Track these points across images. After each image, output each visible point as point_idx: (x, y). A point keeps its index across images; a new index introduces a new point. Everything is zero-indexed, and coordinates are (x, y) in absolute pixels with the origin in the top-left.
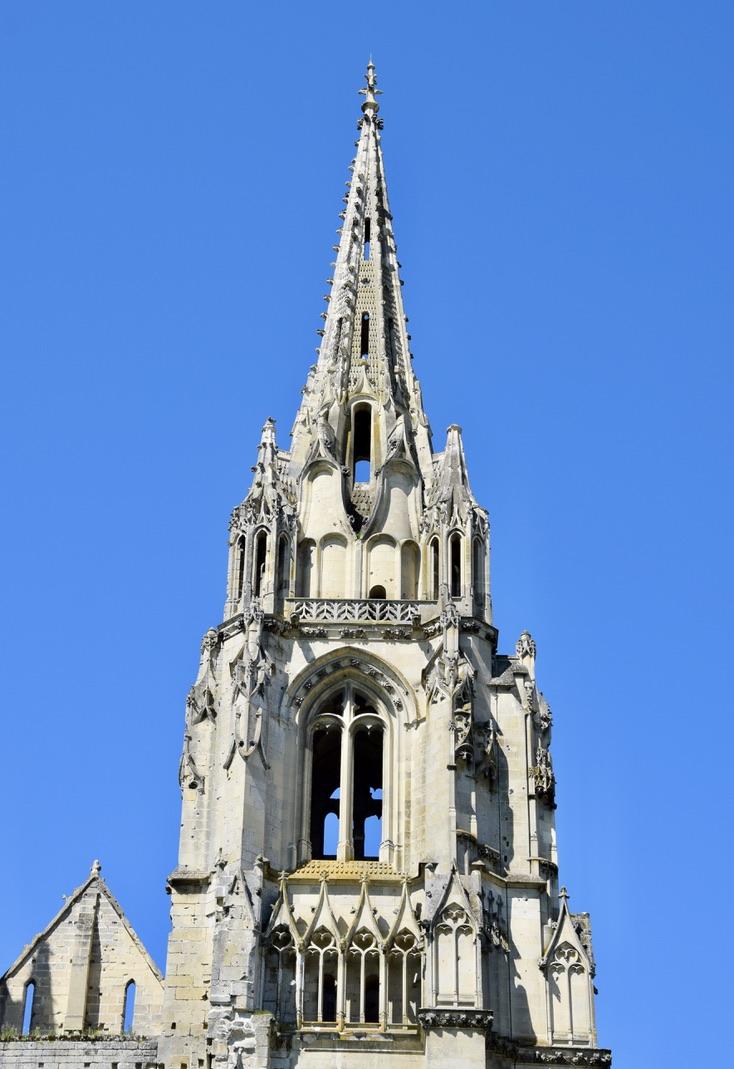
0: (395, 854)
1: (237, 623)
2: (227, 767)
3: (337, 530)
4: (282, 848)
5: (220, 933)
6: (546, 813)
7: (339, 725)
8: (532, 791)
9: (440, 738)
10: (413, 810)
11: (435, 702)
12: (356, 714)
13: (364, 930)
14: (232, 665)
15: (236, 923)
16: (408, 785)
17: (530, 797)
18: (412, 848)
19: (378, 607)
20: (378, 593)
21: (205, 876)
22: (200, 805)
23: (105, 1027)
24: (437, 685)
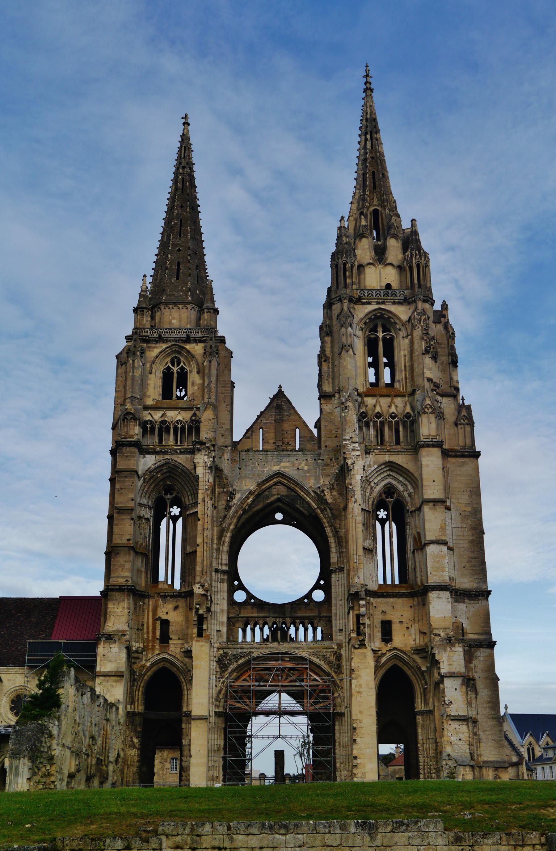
2: (340, 354)
3: (371, 261)
6: (455, 369)
8: (450, 361)
13: (393, 413)
14: (338, 316)
15: (350, 412)
16: (405, 360)
17: (449, 364)
18: (408, 383)
19: (390, 292)
20: (388, 286)
22: (329, 368)
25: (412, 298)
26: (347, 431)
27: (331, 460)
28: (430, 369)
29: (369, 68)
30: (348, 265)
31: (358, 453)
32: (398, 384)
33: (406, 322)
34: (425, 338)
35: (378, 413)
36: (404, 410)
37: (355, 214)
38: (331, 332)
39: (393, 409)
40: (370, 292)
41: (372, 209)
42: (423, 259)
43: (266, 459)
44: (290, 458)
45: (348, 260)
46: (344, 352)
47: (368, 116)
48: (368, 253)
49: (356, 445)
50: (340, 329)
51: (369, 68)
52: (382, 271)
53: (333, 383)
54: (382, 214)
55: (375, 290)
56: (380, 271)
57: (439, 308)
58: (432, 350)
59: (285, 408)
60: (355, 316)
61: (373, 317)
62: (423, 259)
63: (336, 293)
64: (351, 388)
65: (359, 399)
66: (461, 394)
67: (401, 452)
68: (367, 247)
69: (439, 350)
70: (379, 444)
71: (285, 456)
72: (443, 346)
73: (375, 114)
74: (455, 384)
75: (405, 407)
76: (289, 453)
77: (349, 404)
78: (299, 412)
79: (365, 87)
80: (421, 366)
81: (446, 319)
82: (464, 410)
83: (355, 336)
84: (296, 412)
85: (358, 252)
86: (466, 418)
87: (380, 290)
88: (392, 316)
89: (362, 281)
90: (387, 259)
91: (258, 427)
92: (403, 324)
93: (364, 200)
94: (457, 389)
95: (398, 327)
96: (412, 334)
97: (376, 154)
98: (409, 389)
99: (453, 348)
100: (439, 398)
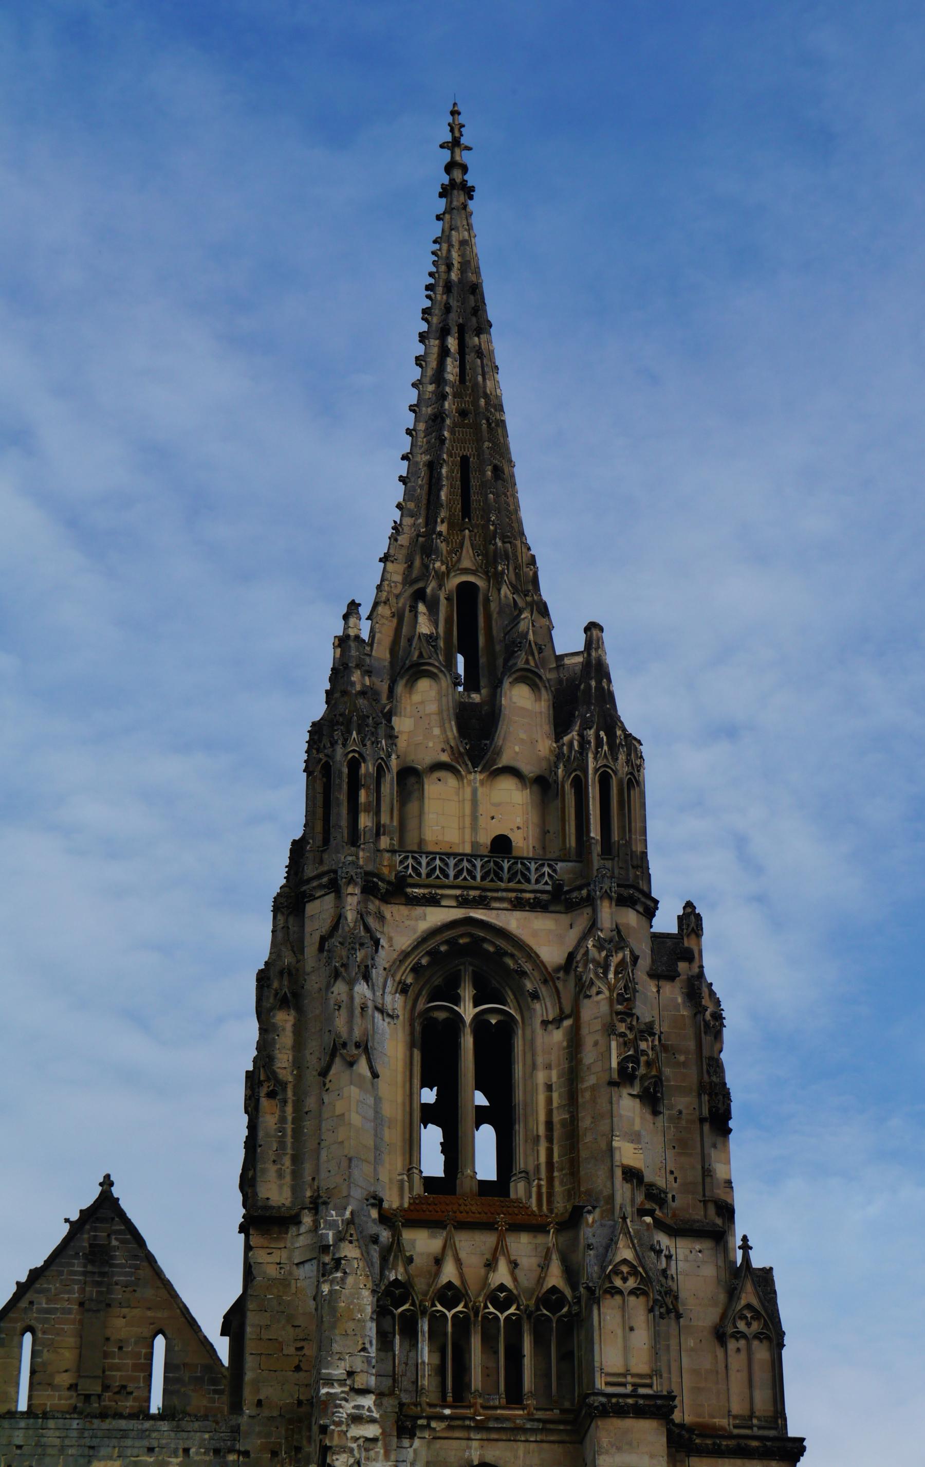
0: (534, 1190)
1: (325, 880)
2: (324, 1073)
3: (445, 758)
4: (390, 1180)
5: (330, 1292)
6: (719, 1140)
7: (459, 1018)
8: (705, 1112)
9: (596, 1044)
10: (556, 1134)
11: (589, 997)
12: (475, 1006)
13: (502, 1287)
14: (323, 940)
15: (350, 1280)
16: (549, 1101)
17: (702, 1120)
18: (557, 1183)
19: (506, 865)
20: (501, 844)
21: (293, 1212)
22: (282, 1120)
23: (129, 1389)
24: (592, 976)
25: (580, 888)
26: (336, 1347)
27: (274, 1454)
28: (635, 1138)
29: (461, 119)
30: (367, 768)
31: (372, 1431)
32: (521, 1186)
33: (558, 969)
34: (622, 1028)
35: (450, 1285)
36: (541, 1280)
37: (398, 597)
38: (296, 995)
39: (502, 1275)
40: (438, 862)
41: (455, 581)
42: (622, 757)
43: (38, 1445)
44: (129, 1442)
45: (368, 751)
46: (338, 1066)
47: (454, 276)
48: (437, 731)
49: (368, 1401)
50: (329, 986)
51: (461, 119)
52: (480, 791)
53: (296, 1174)
54: (487, 601)
55: (455, 855)
56: (474, 792)
57: (672, 928)
58: (642, 1070)
59: (120, 1258)
60: (383, 942)
61: (443, 948)
62: (622, 757)
63: (321, 862)
64: (357, 1194)
65: (385, 1235)
66: (741, 1227)
67: (524, 1430)
68: (432, 708)
69: (667, 1071)
70: (450, 1399)
71: (109, 1434)
72: (682, 1058)
73: (477, 272)
74: (720, 1193)
75: (544, 1267)
76: (123, 1424)
77: (350, 1251)
78: (169, 1274)
79: (446, 179)
80: (604, 1127)
81: (696, 965)
82: (749, 1286)
83: (381, 1011)
84: (158, 1273)
85: (402, 724)
86: (757, 1316)
87: (470, 858)
88: (510, 949)
89: (412, 824)
90: (498, 753)
91: (19, 1326)
92: (548, 977)
93: (428, 550)
94: (727, 1212)
95: (529, 986)
96: (575, 1013)
97: (475, 403)
98: (561, 1205)
99: (716, 1067)
100: (664, 1240)
